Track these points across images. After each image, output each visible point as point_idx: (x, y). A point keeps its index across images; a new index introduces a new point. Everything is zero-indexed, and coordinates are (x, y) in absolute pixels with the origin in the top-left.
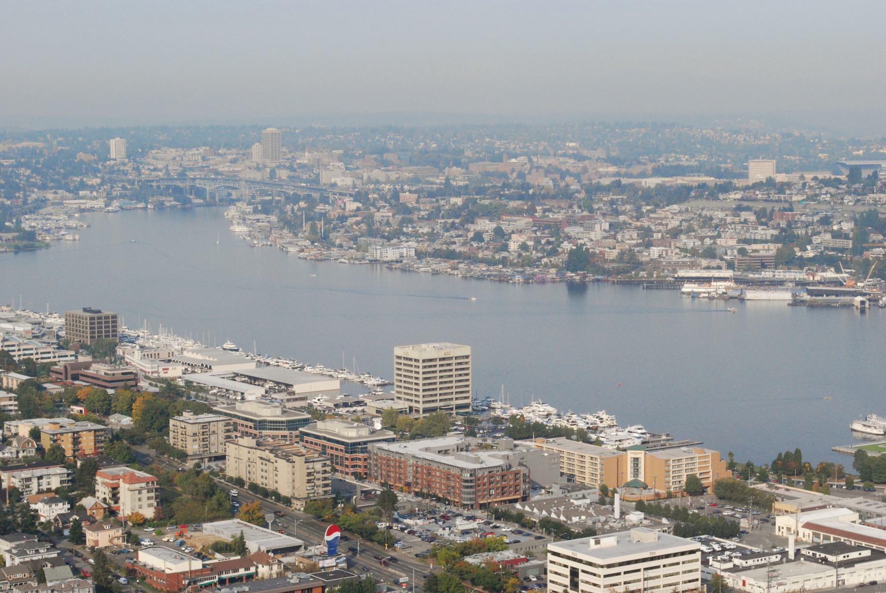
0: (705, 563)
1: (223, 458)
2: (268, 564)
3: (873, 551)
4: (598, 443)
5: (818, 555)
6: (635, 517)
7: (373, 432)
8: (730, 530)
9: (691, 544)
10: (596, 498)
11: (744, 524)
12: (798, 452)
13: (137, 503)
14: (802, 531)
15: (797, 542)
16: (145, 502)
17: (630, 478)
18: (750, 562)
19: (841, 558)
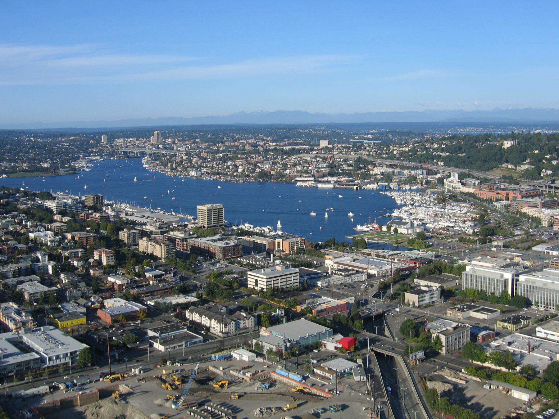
1: (138, 245)
2: (153, 280)
3: (357, 271)
5: (339, 273)
7: (190, 234)
9: (297, 270)
13: (108, 261)
15: (332, 269)
16: (111, 260)
19: (346, 273)
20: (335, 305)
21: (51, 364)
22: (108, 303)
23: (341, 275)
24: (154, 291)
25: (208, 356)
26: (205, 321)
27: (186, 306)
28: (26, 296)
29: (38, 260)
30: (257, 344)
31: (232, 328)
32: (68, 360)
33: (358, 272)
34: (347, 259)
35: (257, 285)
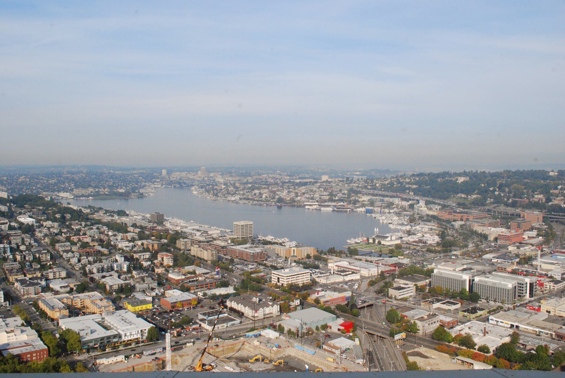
0: (311, 275)
1: (190, 250)
4: (285, 246)
6: (294, 264)
7: (228, 243)
8: (317, 267)
9: (308, 271)
10: (284, 259)
11: (321, 266)
12: (334, 247)
14: (335, 267)
15: (333, 270)
16: (170, 261)
17: (292, 254)
18: (322, 275)
19: (344, 274)
20: (337, 297)
21: (127, 339)
22: (169, 293)
23: (340, 274)
24: (203, 285)
25: (244, 334)
26: (239, 307)
27: (227, 296)
28: (108, 288)
29: (116, 261)
30: (280, 325)
31: (260, 314)
32: (139, 336)
33: (353, 273)
34: (344, 263)
35: (279, 281)
